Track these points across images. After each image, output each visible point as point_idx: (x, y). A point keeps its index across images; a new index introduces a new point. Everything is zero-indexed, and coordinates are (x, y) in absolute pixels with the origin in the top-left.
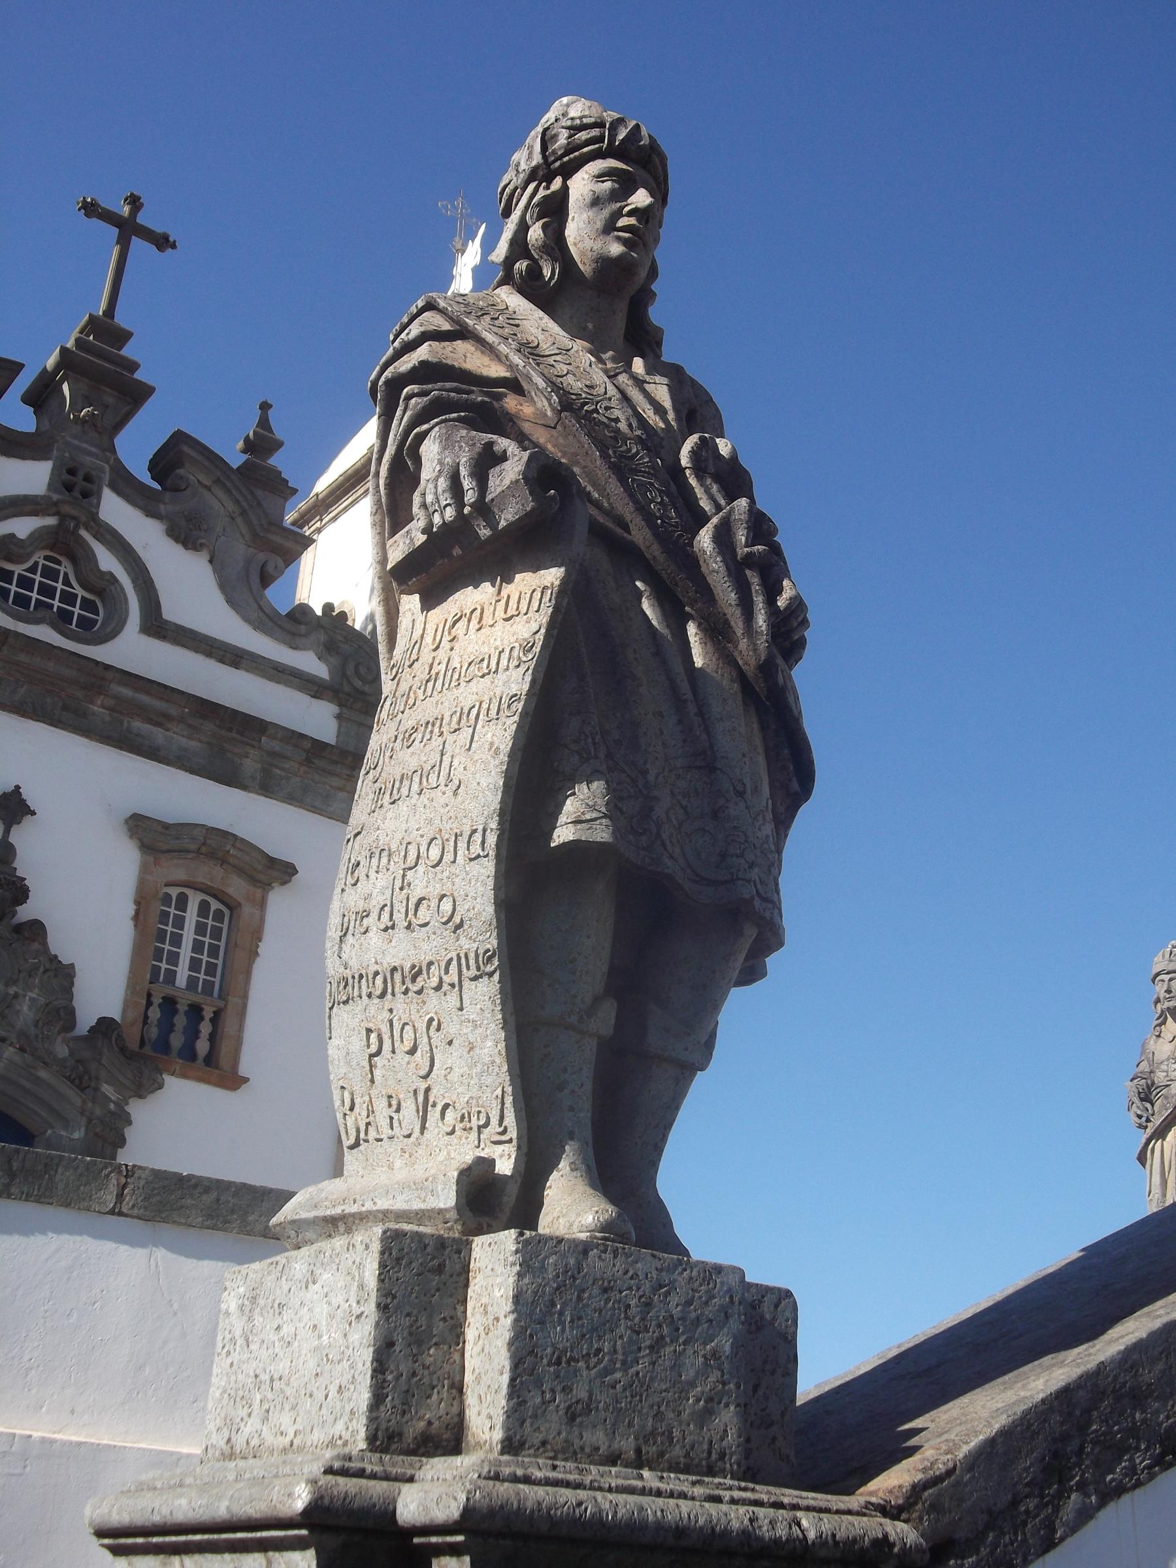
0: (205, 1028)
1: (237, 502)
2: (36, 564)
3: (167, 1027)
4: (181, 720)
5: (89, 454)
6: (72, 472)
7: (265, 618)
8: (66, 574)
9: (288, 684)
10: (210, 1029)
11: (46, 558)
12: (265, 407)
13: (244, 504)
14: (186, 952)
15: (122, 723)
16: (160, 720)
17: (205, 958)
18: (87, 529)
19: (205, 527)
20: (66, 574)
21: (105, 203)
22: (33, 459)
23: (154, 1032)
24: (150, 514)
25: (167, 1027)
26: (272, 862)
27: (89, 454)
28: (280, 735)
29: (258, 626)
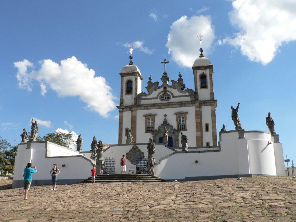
0: (184, 126)
3: (181, 127)
6: (164, 87)
12: (180, 72)
16: (175, 104)
21: (163, 62)
23: (180, 128)
25: (181, 127)
26: (185, 112)
29: (182, 93)
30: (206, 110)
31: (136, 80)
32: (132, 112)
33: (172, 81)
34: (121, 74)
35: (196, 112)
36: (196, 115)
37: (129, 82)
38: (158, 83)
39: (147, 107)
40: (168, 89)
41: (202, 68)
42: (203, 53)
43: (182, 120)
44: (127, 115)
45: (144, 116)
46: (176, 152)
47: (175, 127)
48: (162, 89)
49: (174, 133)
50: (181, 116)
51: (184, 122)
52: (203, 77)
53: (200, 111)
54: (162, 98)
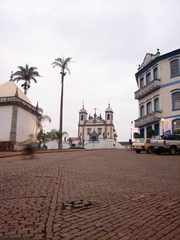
30: (109, 128)
31: (85, 115)
32: (83, 127)
35: (105, 128)
36: (105, 129)
37: (82, 116)
38: (92, 117)
39: (88, 125)
40: (96, 119)
44: (81, 128)
45: (87, 129)
46: (91, 143)
47: (98, 133)
49: (97, 135)
50: (100, 129)
52: (109, 115)
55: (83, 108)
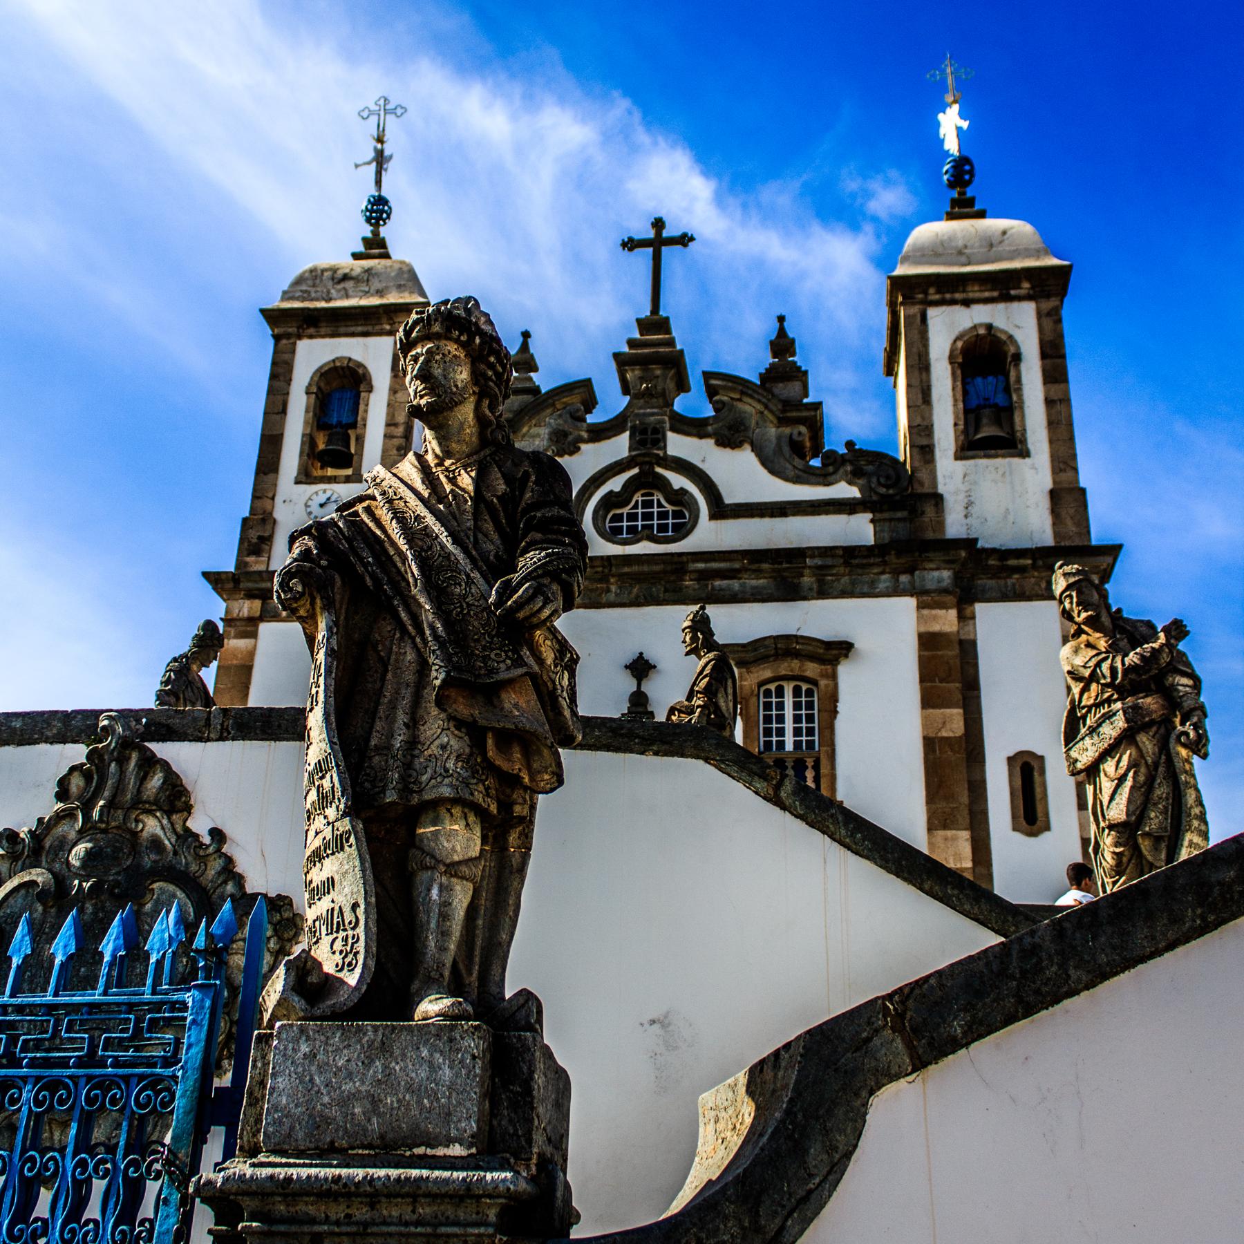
0: (810, 774)
1: (759, 401)
2: (637, 501)
4: (746, 570)
5: (653, 414)
6: (644, 431)
7: (800, 473)
8: (658, 500)
9: (827, 513)
10: (813, 774)
11: (643, 495)
12: (781, 319)
13: (764, 400)
14: (789, 725)
15: (707, 586)
17: (804, 725)
18: (659, 466)
19: (742, 428)
20: (658, 500)
22: (615, 435)
24: (701, 436)
26: (829, 645)
27: (653, 414)
28: (816, 553)
29: (796, 480)
33: (707, 375)
34: (272, 317)
35: (928, 642)
40: (678, 445)
41: (974, 292)
42: (970, 192)
43: (789, 712)
48: (620, 446)
51: (810, 732)
53: (961, 642)
54: (618, 518)
55: (375, 246)
